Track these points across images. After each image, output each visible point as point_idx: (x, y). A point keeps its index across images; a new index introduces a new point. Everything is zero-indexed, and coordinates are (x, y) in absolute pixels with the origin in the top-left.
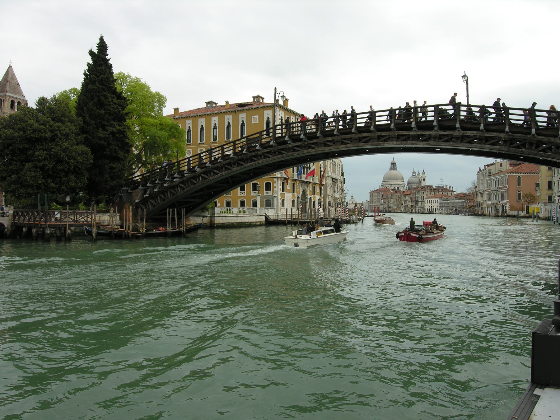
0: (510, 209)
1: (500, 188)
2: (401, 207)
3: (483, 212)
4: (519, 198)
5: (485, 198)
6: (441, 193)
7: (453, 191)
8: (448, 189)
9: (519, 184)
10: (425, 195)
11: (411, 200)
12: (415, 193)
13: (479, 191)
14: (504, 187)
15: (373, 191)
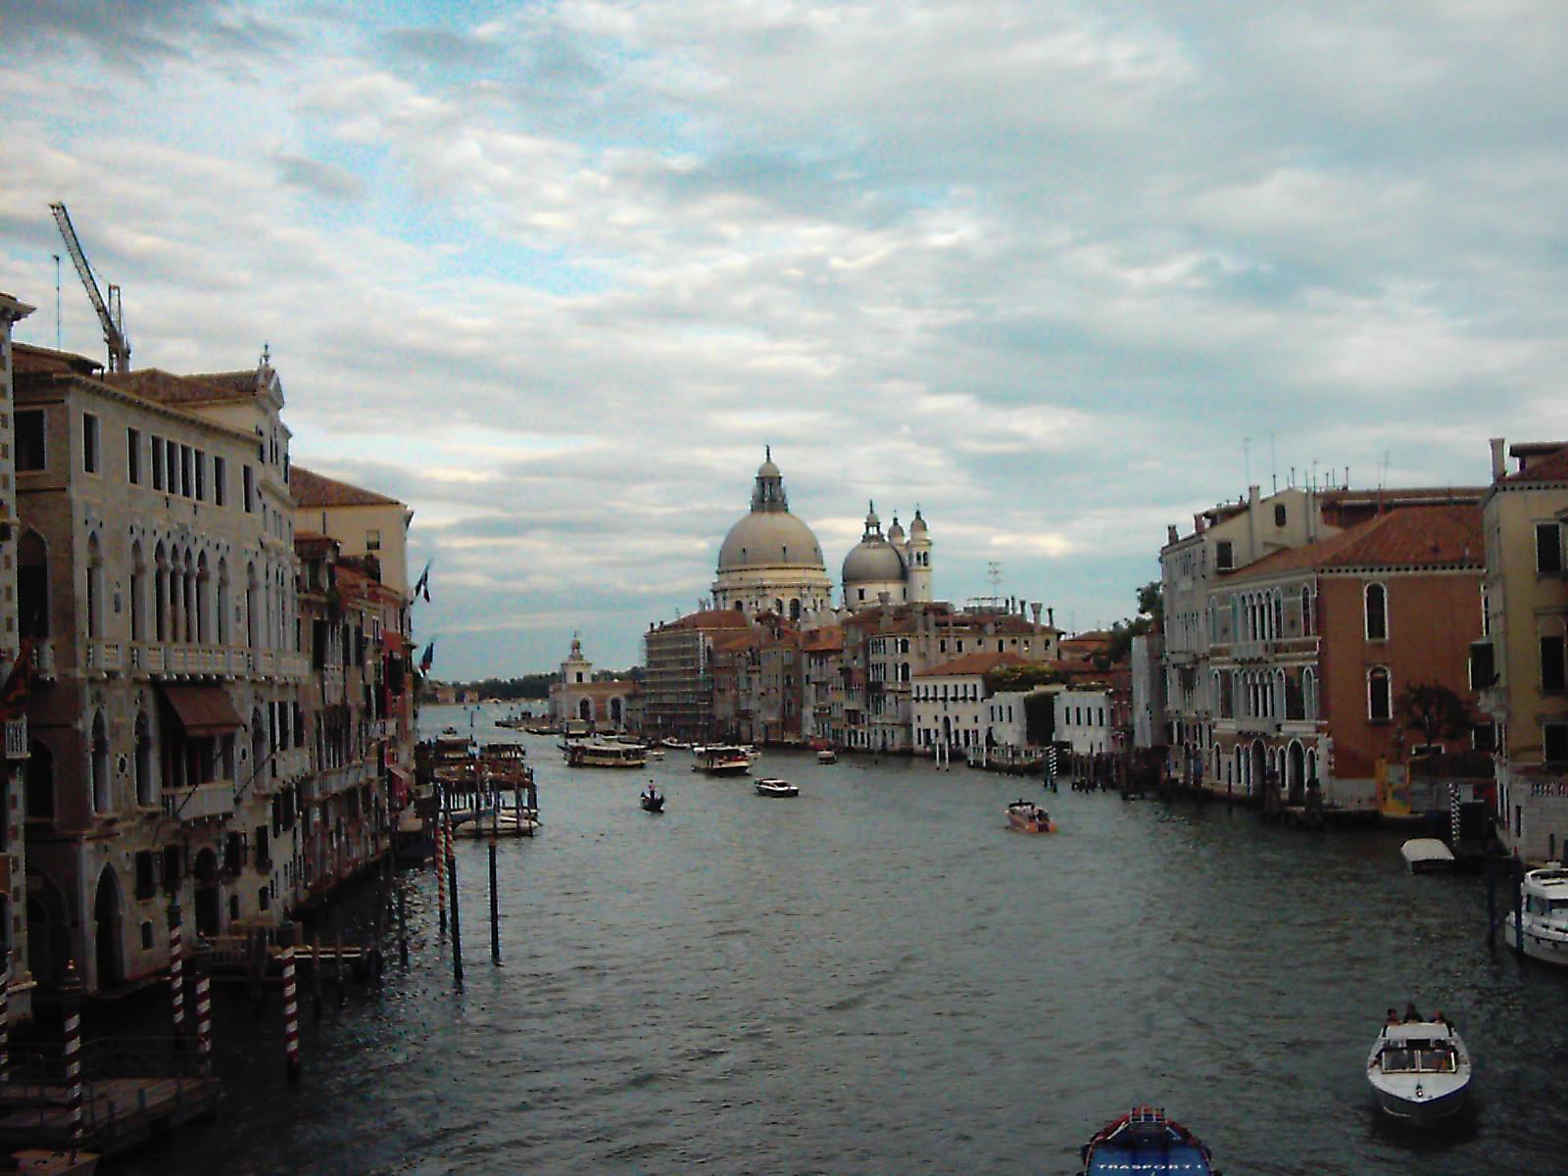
0: (1337, 773)
1: (1278, 648)
2: (799, 714)
3: (1198, 776)
4: (1380, 707)
5: (1206, 697)
6: (991, 645)
7: (1049, 630)
8: (1030, 620)
9: (1376, 629)
10: (911, 658)
11: (848, 685)
12: (865, 646)
13: (1175, 659)
14: (1299, 647)
15: (663, 627)
